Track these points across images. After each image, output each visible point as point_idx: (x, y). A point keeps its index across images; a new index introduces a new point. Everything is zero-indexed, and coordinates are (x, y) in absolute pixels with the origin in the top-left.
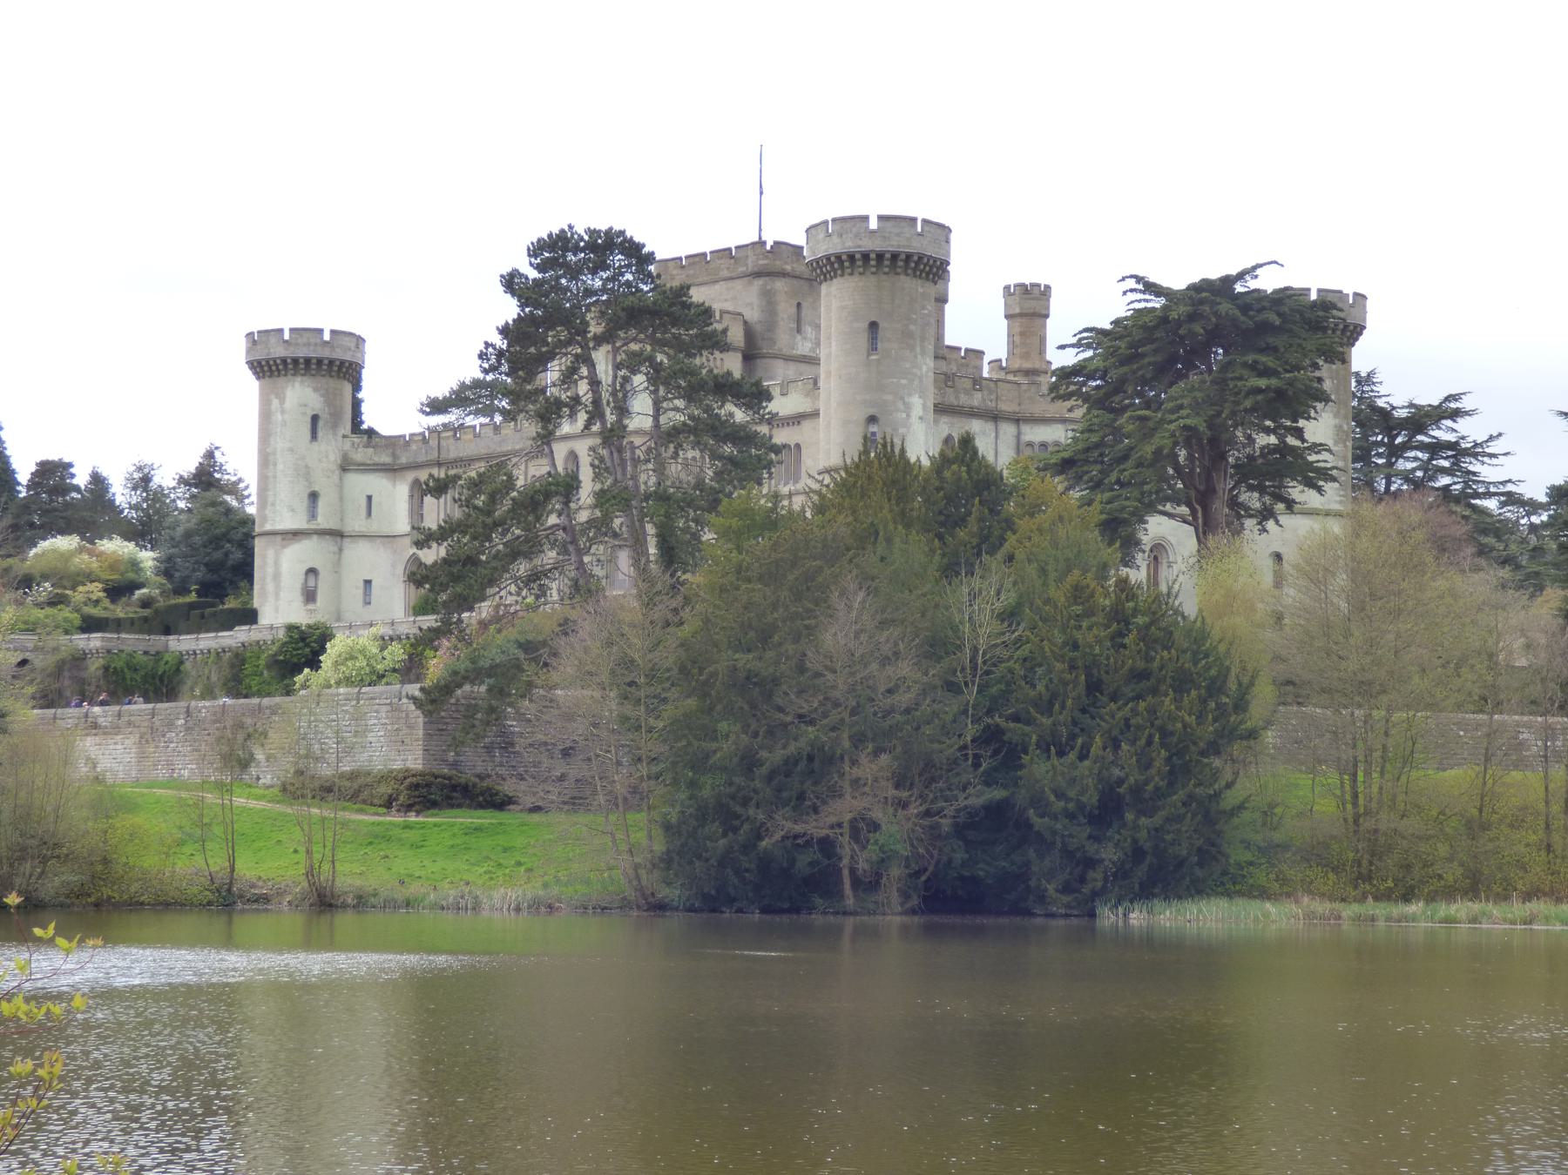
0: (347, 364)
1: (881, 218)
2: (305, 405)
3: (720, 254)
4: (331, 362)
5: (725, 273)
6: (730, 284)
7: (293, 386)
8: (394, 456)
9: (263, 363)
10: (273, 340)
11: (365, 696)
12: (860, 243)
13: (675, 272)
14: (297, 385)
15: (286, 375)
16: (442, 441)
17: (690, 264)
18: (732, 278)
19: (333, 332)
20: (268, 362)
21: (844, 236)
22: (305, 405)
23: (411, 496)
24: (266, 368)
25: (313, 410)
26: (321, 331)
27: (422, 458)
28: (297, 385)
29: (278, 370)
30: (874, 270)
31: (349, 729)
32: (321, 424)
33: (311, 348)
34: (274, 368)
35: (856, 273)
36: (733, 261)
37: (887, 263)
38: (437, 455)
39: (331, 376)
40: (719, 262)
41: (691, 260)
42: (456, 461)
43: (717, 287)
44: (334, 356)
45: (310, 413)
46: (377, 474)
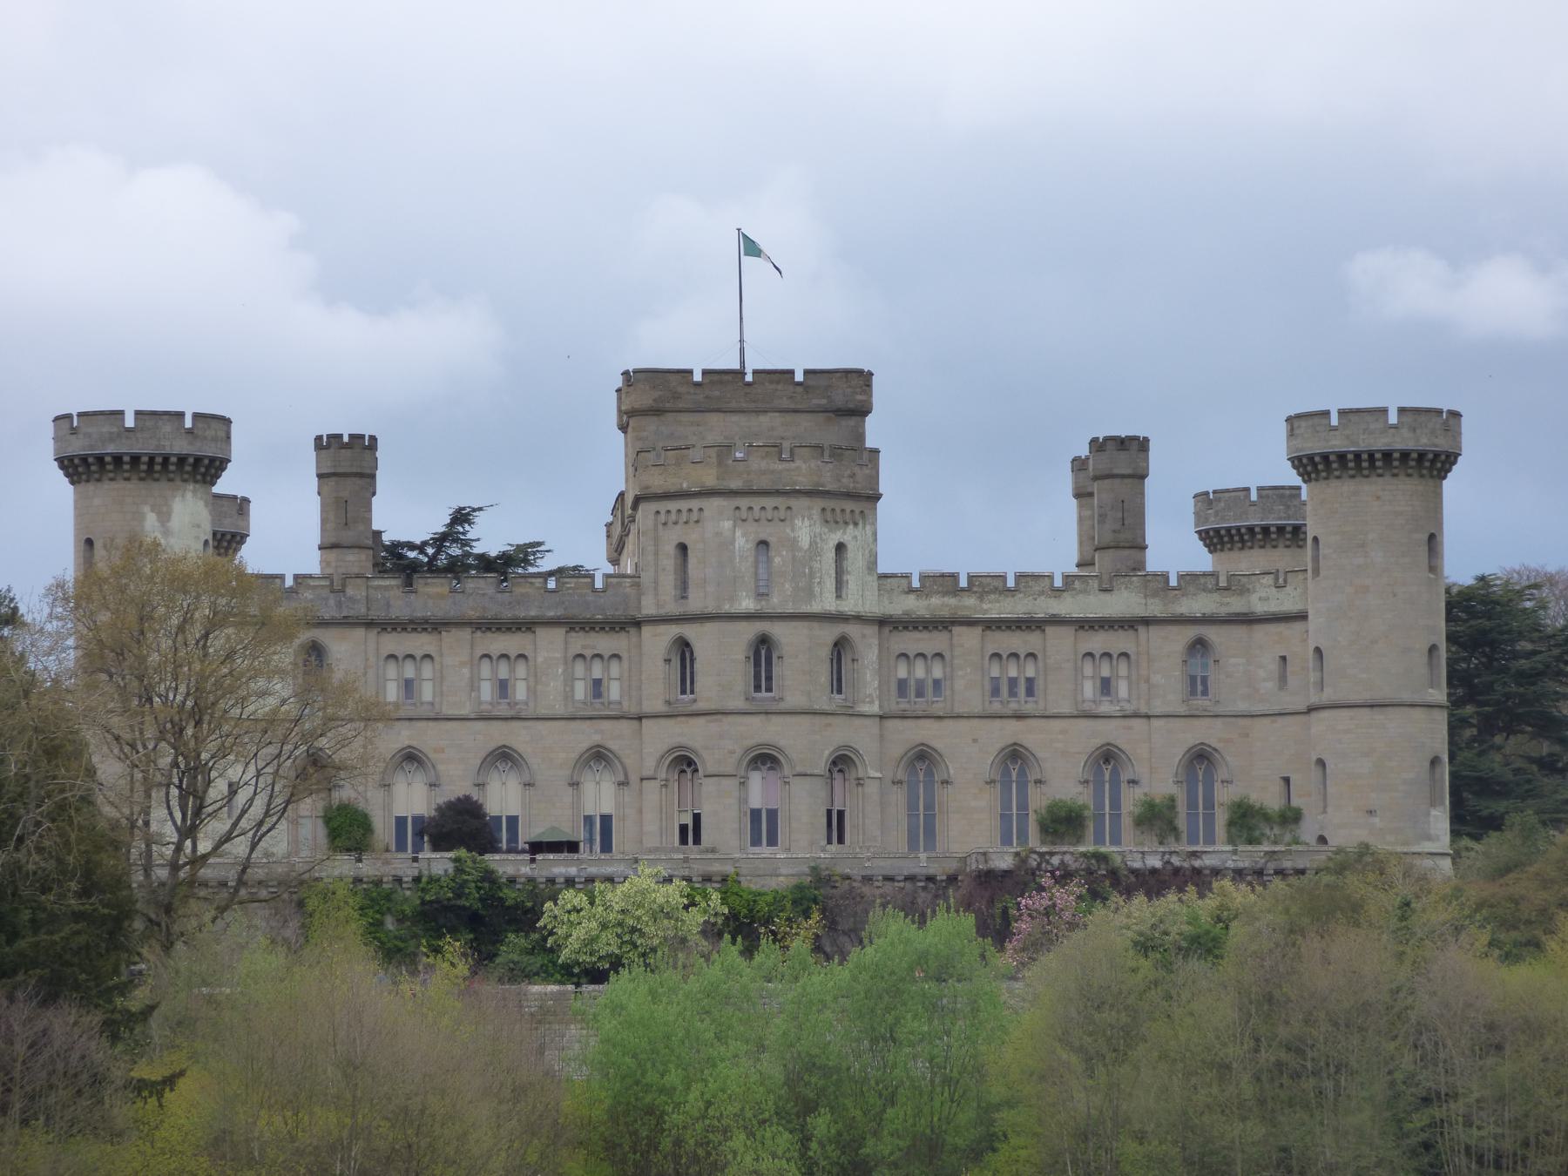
2: (199, 526)
4: (198, 460)
5: (786, 404)
6: (789, 417)
7: (183, 496)
10: (167, 428)
12: (1437, 441)
13: (681, 389)
14: (189, 495)
17: (712, 383)
18: (796, 411)
20: (152, 459)
21: (1418, 431)
27: (329, 611)
28: (189, 495)
34: (158, 468)
36: (800, 389)
38: (363, 610)
40: (773, 386)
41: (716, 377)
42: (411, 621)
43: (765, 420)
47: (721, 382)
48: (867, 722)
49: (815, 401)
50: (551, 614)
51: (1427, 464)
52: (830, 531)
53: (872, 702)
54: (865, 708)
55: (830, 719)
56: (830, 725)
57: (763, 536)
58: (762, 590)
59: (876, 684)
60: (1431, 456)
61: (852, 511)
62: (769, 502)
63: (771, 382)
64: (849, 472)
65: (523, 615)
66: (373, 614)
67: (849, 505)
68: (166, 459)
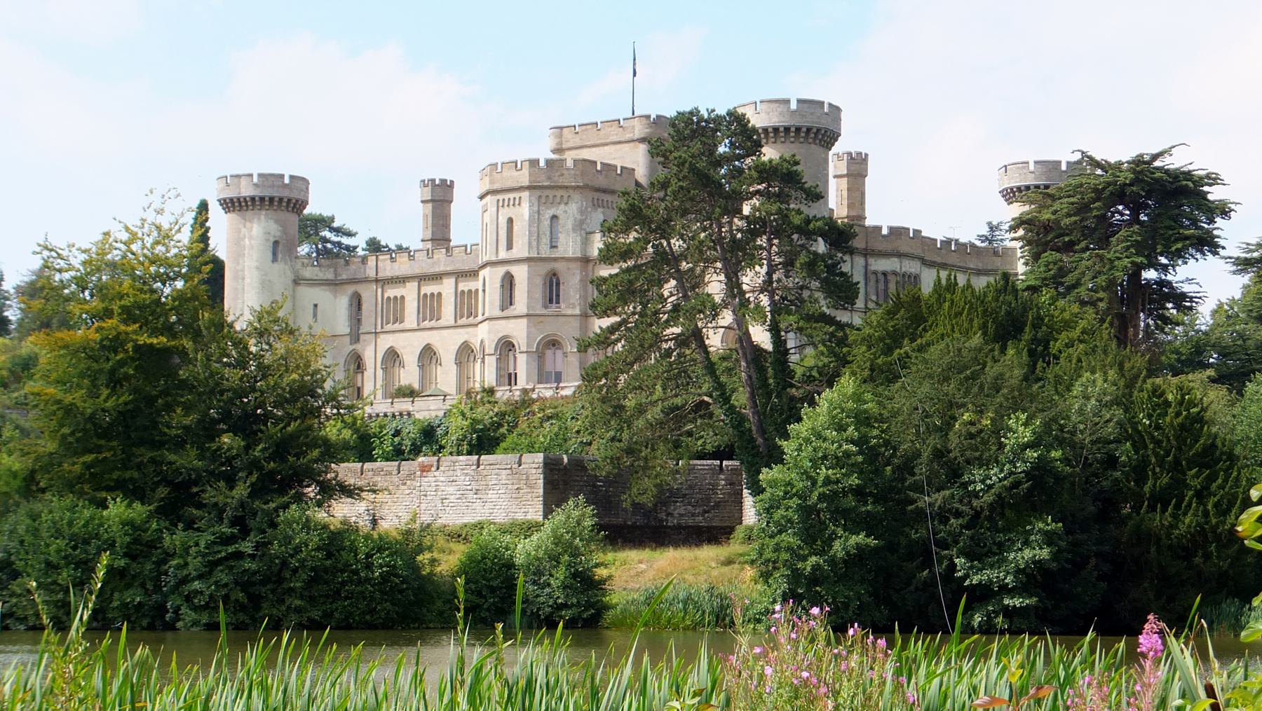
0: (300, 202)
1: (799, 101)
2: (269, 233)
3: (609, 124)
4: (289, 201)
7: (259, 219)
8: (336, 274)
9: (235, 200)
10: (244, 181)
11: (485, 463)
14: (263, 217)
15: (253, 210)
16: (379, 263)
18: (620, 143)
19: (292, 177)
20: (238, 199)
22: (269, 233)
23: (351, 305)
24: (236, 204)
25: (275, 237)
26: (282, 176)
29: (247, 206)
30: (792, 139)
31: (469, 488)
32: (280, 248)
33: (275, 189)
34: (243, 204)
35: (778, 141)
37: (803, 135)
39: (288, 211)
40: (610, 129)
42: (392, 278)
44: (292, 196)
45: (272, 240)
46: (323, 287)
47: (586, 130)
48: (570, 319)
49: (628, 136)
50: (448, 269)
51: (812, 135)
52: (547, 208)
53: (574, 307)
54: (570, 312)
55: (541, 319)
56: (542, 322)
57: (510, 215)
58: (554, 244)
59: (578, 296)
60: (815, 130)
61: (562, 196)
62: (511, 196)
63: (608, 126)
64: (559, 173)
65: (437, 270)
66: (381, 275)
67: (559, 193)
68: (245, 199)
